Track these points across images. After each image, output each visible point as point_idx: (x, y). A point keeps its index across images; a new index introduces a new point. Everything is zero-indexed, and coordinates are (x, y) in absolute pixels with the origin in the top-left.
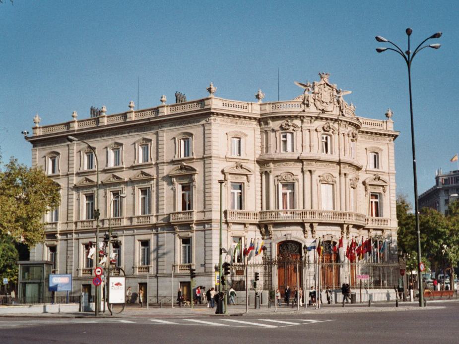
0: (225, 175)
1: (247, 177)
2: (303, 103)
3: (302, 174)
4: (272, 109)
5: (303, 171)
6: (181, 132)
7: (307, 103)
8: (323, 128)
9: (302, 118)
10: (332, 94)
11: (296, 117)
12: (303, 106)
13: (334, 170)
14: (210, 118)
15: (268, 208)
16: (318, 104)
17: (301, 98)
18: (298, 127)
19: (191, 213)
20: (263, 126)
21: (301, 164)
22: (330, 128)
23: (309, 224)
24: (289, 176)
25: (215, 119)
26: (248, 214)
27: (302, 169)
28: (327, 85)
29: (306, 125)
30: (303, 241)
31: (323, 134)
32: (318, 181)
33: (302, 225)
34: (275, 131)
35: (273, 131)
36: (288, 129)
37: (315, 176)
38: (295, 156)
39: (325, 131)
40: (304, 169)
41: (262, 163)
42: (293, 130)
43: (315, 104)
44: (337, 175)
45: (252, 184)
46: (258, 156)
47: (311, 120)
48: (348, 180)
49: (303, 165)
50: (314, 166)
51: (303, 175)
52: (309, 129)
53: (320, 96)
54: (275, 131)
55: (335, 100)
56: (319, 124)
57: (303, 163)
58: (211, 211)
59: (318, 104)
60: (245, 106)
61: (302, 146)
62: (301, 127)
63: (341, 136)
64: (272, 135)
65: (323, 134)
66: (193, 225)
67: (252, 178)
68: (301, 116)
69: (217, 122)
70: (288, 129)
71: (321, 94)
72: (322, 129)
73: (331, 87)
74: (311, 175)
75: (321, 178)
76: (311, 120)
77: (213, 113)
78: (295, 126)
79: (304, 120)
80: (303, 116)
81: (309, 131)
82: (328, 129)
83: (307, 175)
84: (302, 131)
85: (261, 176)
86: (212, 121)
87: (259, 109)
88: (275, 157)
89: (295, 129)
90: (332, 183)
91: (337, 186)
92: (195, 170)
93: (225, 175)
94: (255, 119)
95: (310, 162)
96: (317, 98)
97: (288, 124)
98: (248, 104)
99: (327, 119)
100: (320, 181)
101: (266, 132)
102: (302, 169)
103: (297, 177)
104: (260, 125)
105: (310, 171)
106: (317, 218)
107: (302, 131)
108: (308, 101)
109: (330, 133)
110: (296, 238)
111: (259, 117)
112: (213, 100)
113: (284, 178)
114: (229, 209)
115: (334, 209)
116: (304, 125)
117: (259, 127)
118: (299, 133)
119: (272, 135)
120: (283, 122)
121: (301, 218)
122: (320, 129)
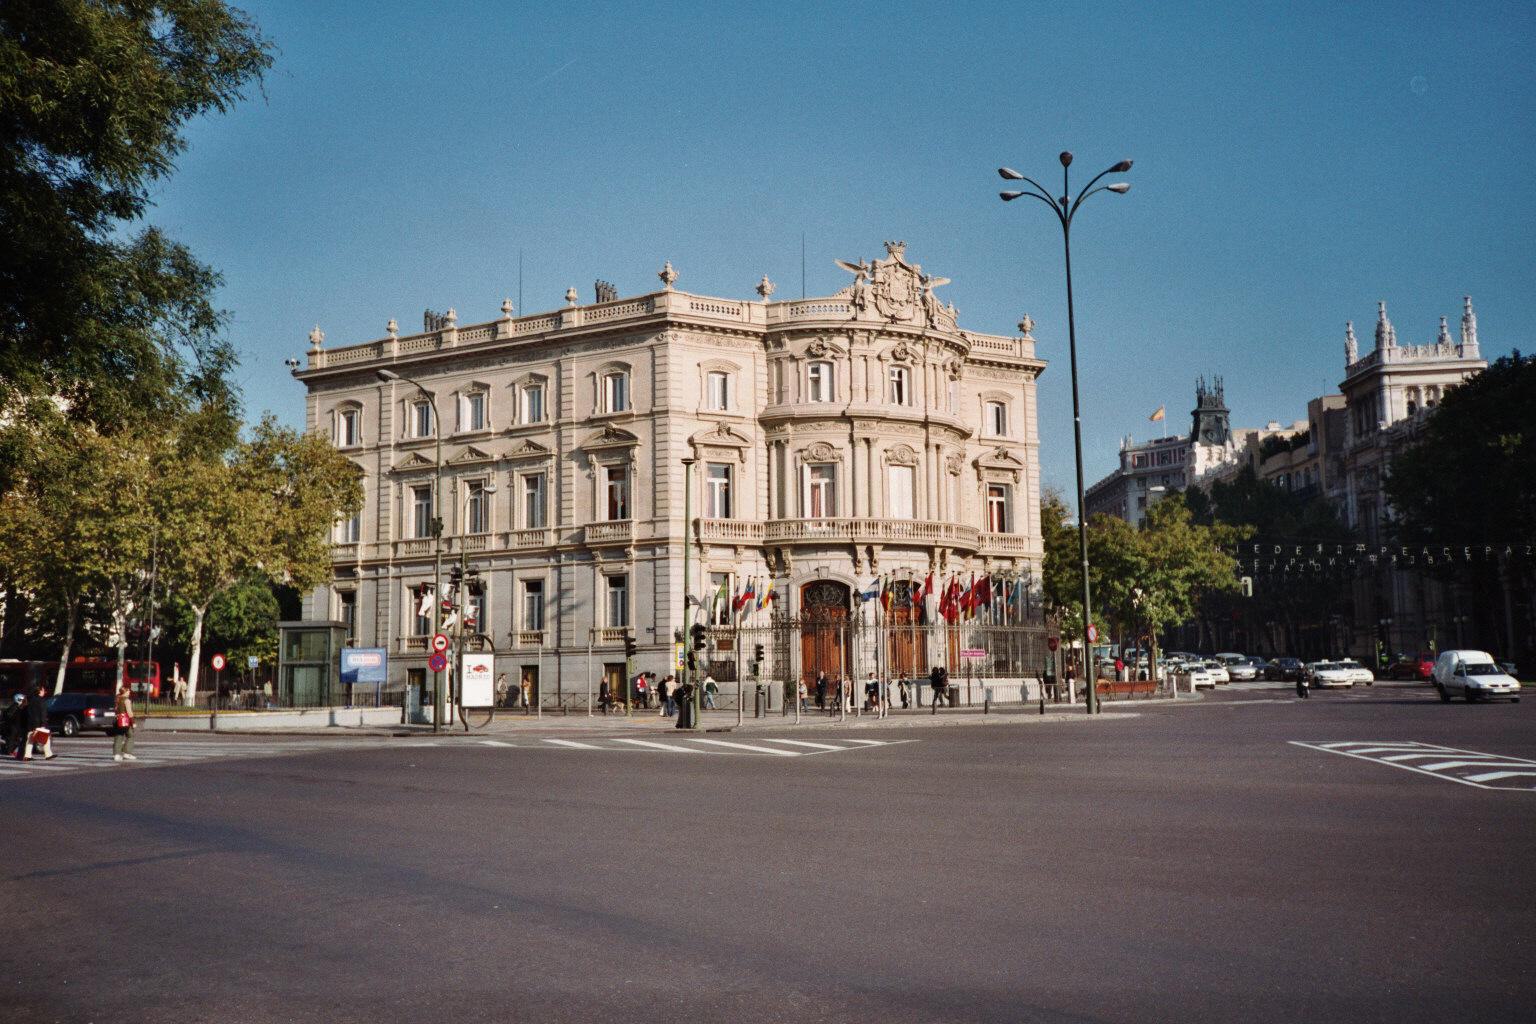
0: (695, 448)
1: (740, 452)
2: (853, 303)
3: (850, 446)
4: (789, 315)
5: (852, 441)
6: (606, 360)
7: (861, 302)
8: (893, 353)
9: (850, 333)
10: (910, 284)
11: (839, 331)
12: (852, 308)
13: (916, 438)
14: (664, 334)
15: (782, 514)
16: (883, 304)
17: (848, 294)
18: (843, 352)
19: (627, 525)
20: (772, 350)
21: (849, 426)
22: (907, 353)
23: (864, 547)
24: (825, 450)
25: (676, 335)
26: (742, 527)
27: (851, 435)
28: (902, 266)
29: (859, 348)
31: (893, 366)
32: (883, 461)
33: (850, 548)
34: (797, 360)
35: (793, 358)
36: (822, 355)
37: (877, 451)
38: (837, 410)
39: (896, 358)
40: (855, 436)
41: (769, 423)
42: (833, 357)
43: (876, 305)
44: (920, 447)
45: (749, 465)
46: (761, 410)
47: (868, 338)
48: (943, 458)
49: (852, 429)
50: (874, 430)
51: (853, 447)
53: (887, 288)
54: (797, 360)
55: (918, 298)
56: (884, 345)
57: (852, 423)
58: (667, 521)
59: (883, 304)
60: (736, 308)
61: (851, 390)
62: (849, 351)
63: (930, 369)
64: (790, 367)
65: (893, 366)
66: (632, 549)
67: (749, 454)
68: (848, 330)
69: (679, 340)
70: (822, 355)
71: (889, 285)
72: (890, 355)
73: (909, 270)
74: (869, 447)
75: (890, 454)
76: (868, 338)
77: (671, 324)
78: (836, 349)
79: (855, 337)
80: (853, 330)
81: (866, 360)
82: (903, 356)
83: (861, 447)
84: (850, 359)
85: (769, 450)
86: (670, 340)
87: (764, 315)
88: (797, 411)
89: (836, 355)
90: (912, 464)
91: (921, 470)
92: (635, 438)
93: (695, 448)
94: (756, 334)
95: (866, 423)
96: (880, 292)
97: (822, 346)
98: (741, 304)
99: (900, 335)
100: (888, 459)
101: (778, 361)
102: (851, 435)
103: (840, 452)
104: (767, 347)
105: (867, 441)
106: (881, 536)
107: (850, 359)
108: (862, 298)
109: (908, 363)
110: (839, 576)
111: (766, 331)
112: (671, 296)
113: (814, 453)
114: (704, 518)
115: (915, 516)
116: (855, 346)
117: (764, 351)
118: (845, 363)
119: (790, 367)
120: (812, 341)
121: (850, 535)
122: (887, 355)
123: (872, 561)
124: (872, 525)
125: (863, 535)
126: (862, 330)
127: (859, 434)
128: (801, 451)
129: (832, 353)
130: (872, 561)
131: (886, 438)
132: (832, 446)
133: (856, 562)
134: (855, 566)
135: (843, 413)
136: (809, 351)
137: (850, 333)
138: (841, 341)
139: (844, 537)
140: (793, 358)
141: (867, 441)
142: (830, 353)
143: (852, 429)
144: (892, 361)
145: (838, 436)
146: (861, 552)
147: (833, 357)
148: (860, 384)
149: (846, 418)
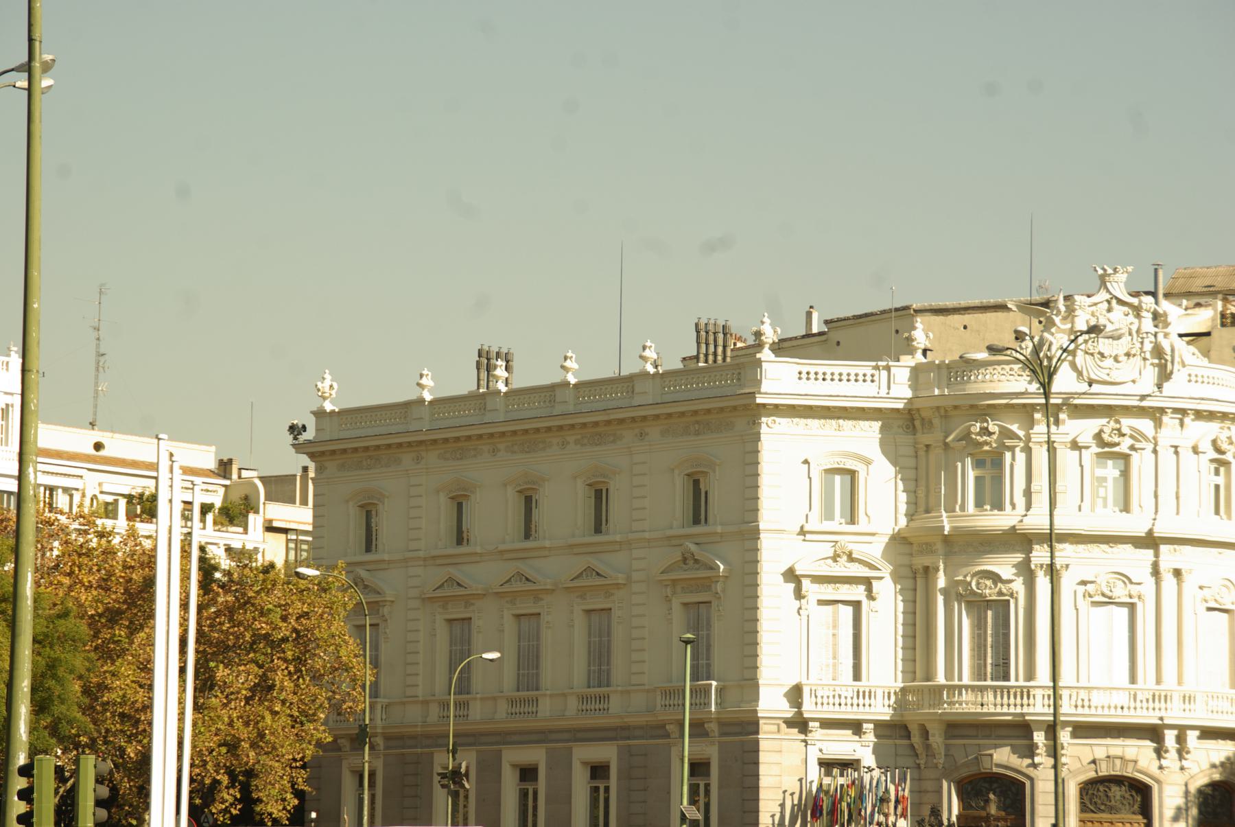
3: (1153, 580)
5: (1156, 572)
8: (1214, 442)
9: (1156, 414)
23: (1175, 732)
30: (1158, 781)
35: (1075, 445)
38: (1136, 524)
49: (1157, 555)
52: (1176, 447)
62: (1155, 438)
64: (1066, 458)
70: (1118, 444)
78: (1137, 435)
80: (1162, 411)
81: (1176, 453)
84: (1155, 451)
89: (1138, 445)
97: (1119, 430)
107: (1155, 451)
118: (1148, 455)
122: (1206, 446)
124: (1188, 699)
127: (1166, 565)
128: (1084, 583)
129: (1131, 442)
132: (1131, 582)
134: (1159, 757)
135: (1150, 532)
136: (1098, 437)
137: (1156, 414)
138: (1145, 425)
140: (1075, 445)
141: (1177, 573)
143: (1157, 555)
146: (1170, 737)
147: (1132, 448)
149: (1150, 541)
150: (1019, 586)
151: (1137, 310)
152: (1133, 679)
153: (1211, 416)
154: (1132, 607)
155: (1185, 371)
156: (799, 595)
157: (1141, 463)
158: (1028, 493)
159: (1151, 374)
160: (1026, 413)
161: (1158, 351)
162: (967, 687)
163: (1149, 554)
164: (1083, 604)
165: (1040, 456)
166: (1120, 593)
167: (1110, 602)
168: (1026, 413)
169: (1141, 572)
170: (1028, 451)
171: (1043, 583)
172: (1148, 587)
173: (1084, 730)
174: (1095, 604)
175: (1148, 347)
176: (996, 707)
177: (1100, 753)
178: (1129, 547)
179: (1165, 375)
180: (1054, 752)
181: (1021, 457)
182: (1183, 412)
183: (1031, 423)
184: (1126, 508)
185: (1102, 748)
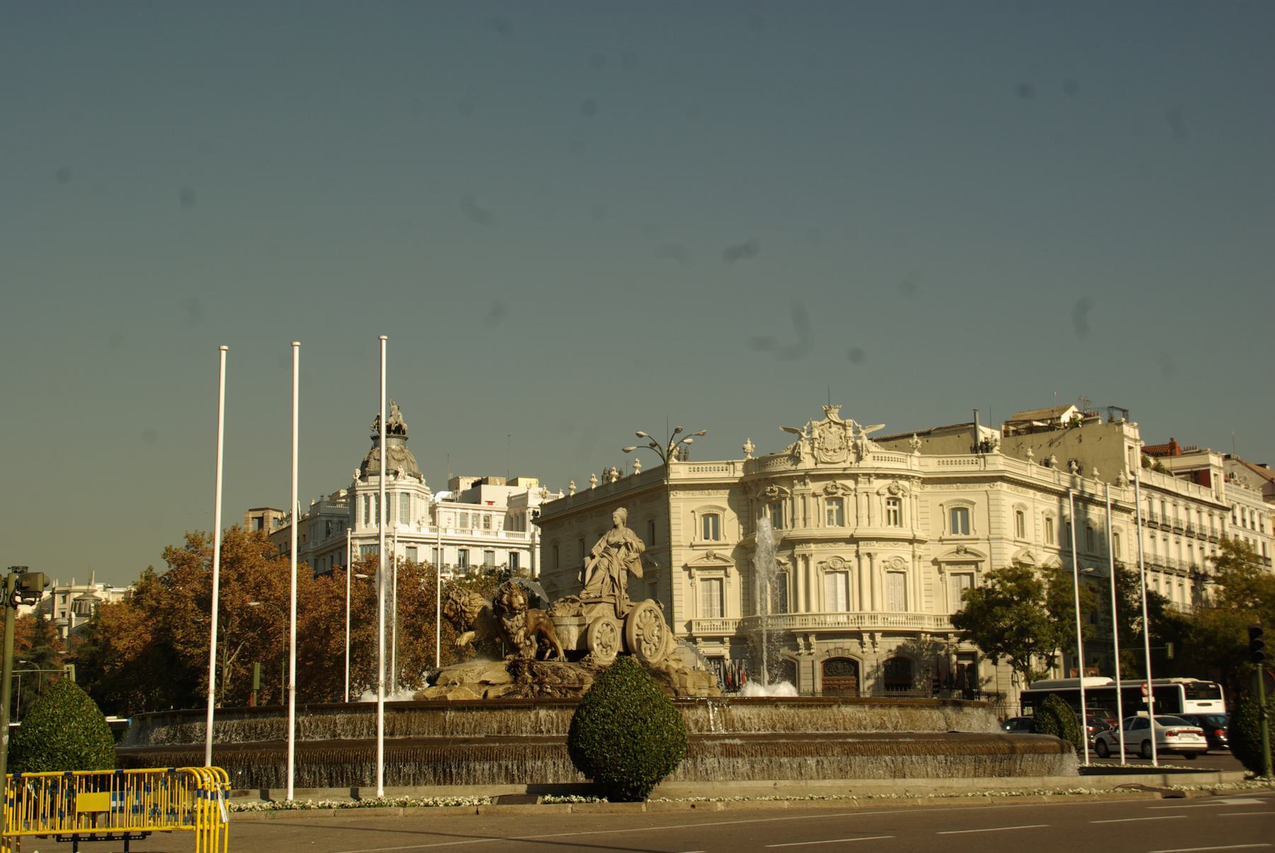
5: (858, 555)
9: (854, 477)
27: (857, 552)
35: (814, 495)
37: (877, 561)
38: (845, 532)
44: (908, 558)
50: (874, 547)
64: (812, 501)
78: (845, 488)
80: (857, 475)
102: (857, 552)
105: (869, 555)
106: (880, 625)
109: (900, 495)
118: (852, 498)
119: (812, 501)
123: (874, 644)
124: (873, 617)
125: (867, 625)
126: (864, 475)
130: (874, 644)
131: (884, 553)
133: (862, 644)
137: (854, 477)
138: (850, 483)
139: (853, 627)
140: (814, 495)
141: (869, 555)
142: (840, 492)
144: (888, 495)
145: (847, 552)
146: (866, 638)
148: (863, 512)
149: (853, 540)
150: (790, 566)
151: (844, 426)
152: (848, 609)
153: (885, 476)
154: (846, 573)
155: (870, 456)
156: (691, 577)
157: (849, 502)
158: (793, 520)
159: (852, 457)
160: (790, 480)
161: (855, 446)
162: (772, 618)
163: (854, 547)
164: (821, 574)
165: (799, 501)
166: (839, 566)
167: (834, 571)
168: (790, 480)
169: (852, 557)
170: (792, 499)
171: (801, 564)
172: (854, 563)
173: (821, 636)
174: (827, 573)
175: (851, 444)
176: (781, 626)
177: (831, 646)
178: (843, 544)
179: (859, 458)
180: (808, 647)
181: (789, 502)
182: (869, 475)
183: (793, 485)
184: (842, 525)
185: (831, 644)
